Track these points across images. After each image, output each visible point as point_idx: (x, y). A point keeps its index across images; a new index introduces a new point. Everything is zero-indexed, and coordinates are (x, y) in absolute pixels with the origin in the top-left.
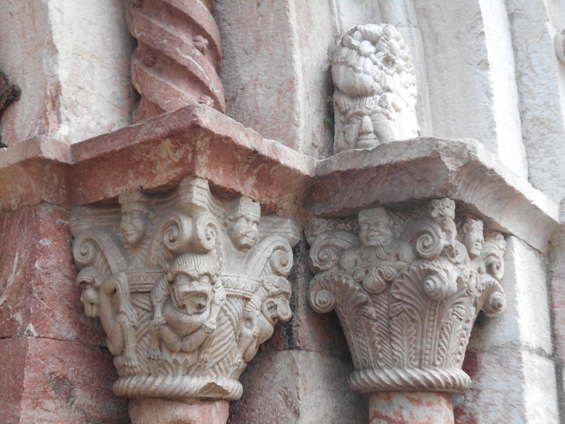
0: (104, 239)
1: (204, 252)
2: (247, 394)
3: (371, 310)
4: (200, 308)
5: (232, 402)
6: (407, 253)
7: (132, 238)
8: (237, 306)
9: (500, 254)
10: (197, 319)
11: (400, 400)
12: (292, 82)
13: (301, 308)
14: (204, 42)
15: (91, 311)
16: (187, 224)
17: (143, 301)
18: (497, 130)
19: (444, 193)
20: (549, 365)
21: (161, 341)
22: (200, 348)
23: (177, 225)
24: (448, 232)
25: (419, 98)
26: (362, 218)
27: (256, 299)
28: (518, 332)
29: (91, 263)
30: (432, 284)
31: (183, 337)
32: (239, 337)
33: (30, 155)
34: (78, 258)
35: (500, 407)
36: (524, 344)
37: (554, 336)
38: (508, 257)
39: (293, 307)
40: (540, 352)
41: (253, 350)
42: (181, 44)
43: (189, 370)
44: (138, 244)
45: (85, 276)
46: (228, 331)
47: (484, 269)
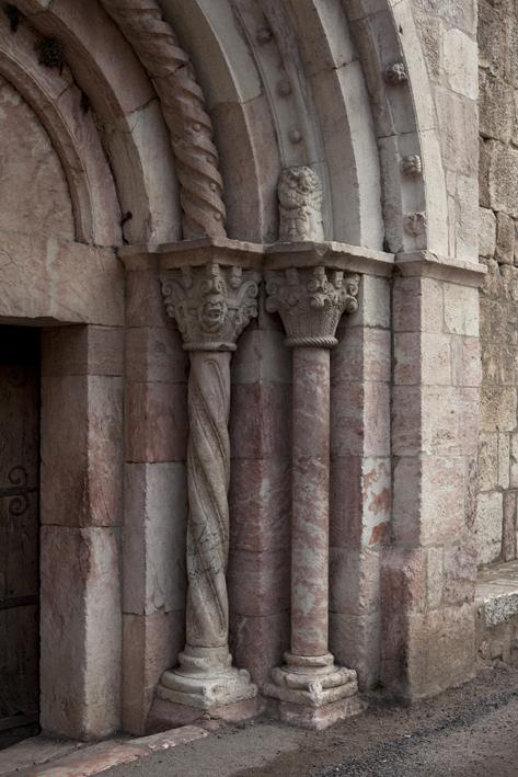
0: (176, 286)
1: (218, 293)
2: (238, 349)
3: (291, 313)
4: (217, 316)
5: (233, 353)
6: (305, 290)
7: (187, 285)
8: (233, 313)
9: (356, 284)
10: (216, 320)
11: (303, 351)
12: (258, 202)
13: (262, 312)
14: (214, 186)
15: (170, 315)
16: (210, 282)
17: (193, 312)
18: (362, 219)
19: (320, 264)
20: (389, 333)
21: (202, 329)
22: (218, 331)
23: (206, 283)
24: (321, 281)
25: (322, 203)
26: (288, 272)
27: (241, 310)
28: (362, 320)
29: (170, 295)
30: (313, 303)
31: (210, 327)
32: (234, 326)
33: (143, 251)
34: (165, 293)
35: (353, 353)
36: (365, 324)
37: (391, 320)
38: (360, 284)
39: (258, 310)
40: (379, 327)
41: (240, 330)
42: (204, 190)
43: (213, 340)
44: (190, 288)
45: (167, 301)
46: (229, 323)
47: (345, 291)
